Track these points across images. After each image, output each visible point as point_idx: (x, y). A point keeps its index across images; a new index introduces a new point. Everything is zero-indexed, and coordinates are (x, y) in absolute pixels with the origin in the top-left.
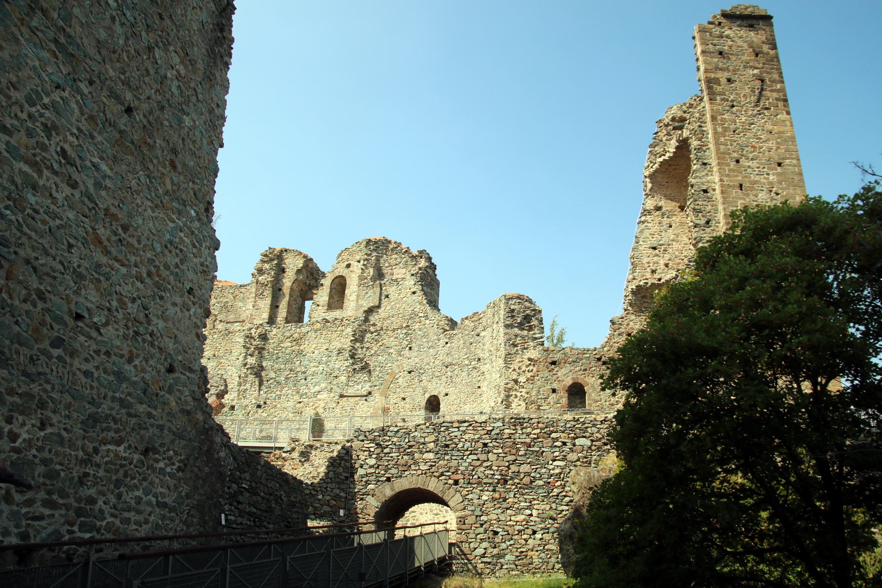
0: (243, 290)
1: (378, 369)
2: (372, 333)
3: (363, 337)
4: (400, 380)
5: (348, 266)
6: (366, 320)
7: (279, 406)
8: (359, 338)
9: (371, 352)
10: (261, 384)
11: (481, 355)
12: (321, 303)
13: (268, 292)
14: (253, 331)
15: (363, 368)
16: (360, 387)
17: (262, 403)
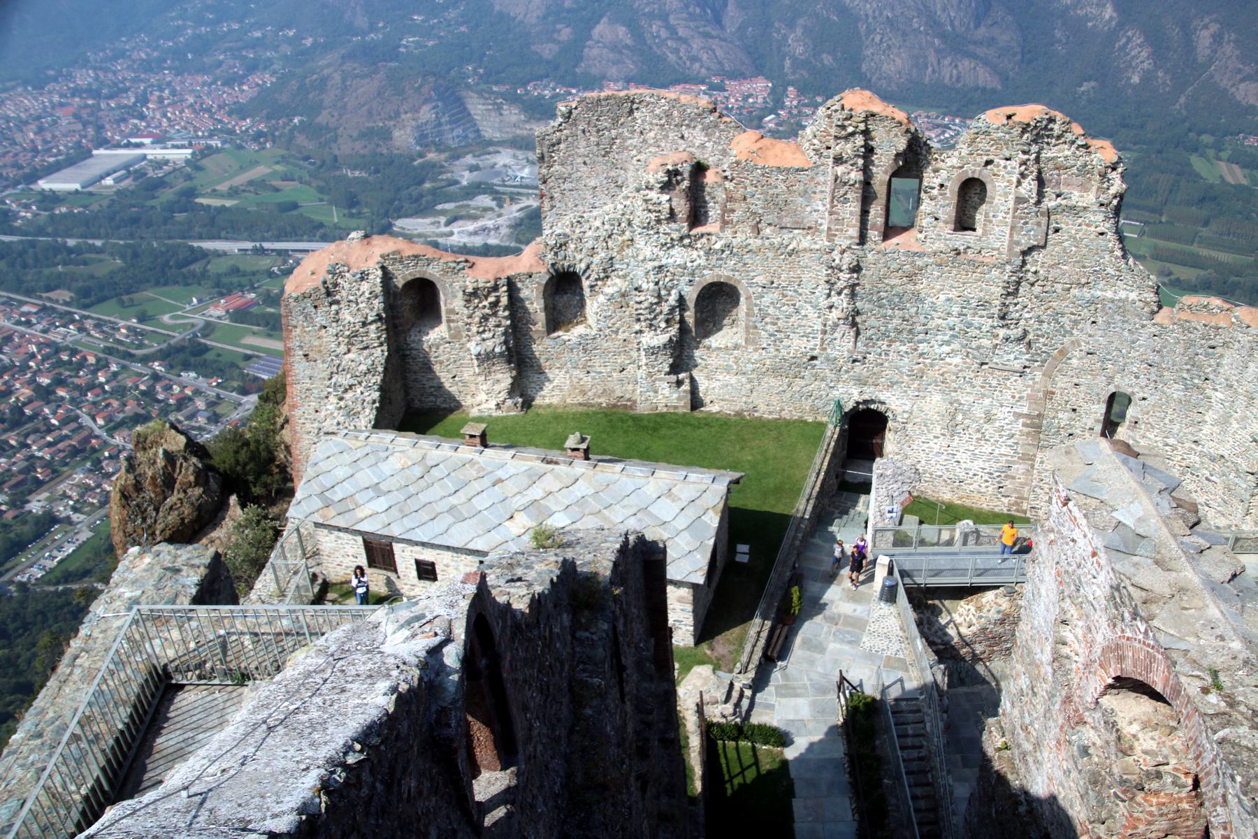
0: (802, 176)
1: (1042, 340)
2: (1032, 285)
3: (1017, 290)
4: (1074, 361)
5: (988, 163)
6: (1024, 263)
7: (886, 364)
8: (1012, 291)
9: (1027, 309)
10: (858, 334)
11: (1211, 376)
12: (943, 217)
13: (854, 196)
14: (836, 255)
15: (1019, 340)
16: (1012, 356)
17: (860, 357)
